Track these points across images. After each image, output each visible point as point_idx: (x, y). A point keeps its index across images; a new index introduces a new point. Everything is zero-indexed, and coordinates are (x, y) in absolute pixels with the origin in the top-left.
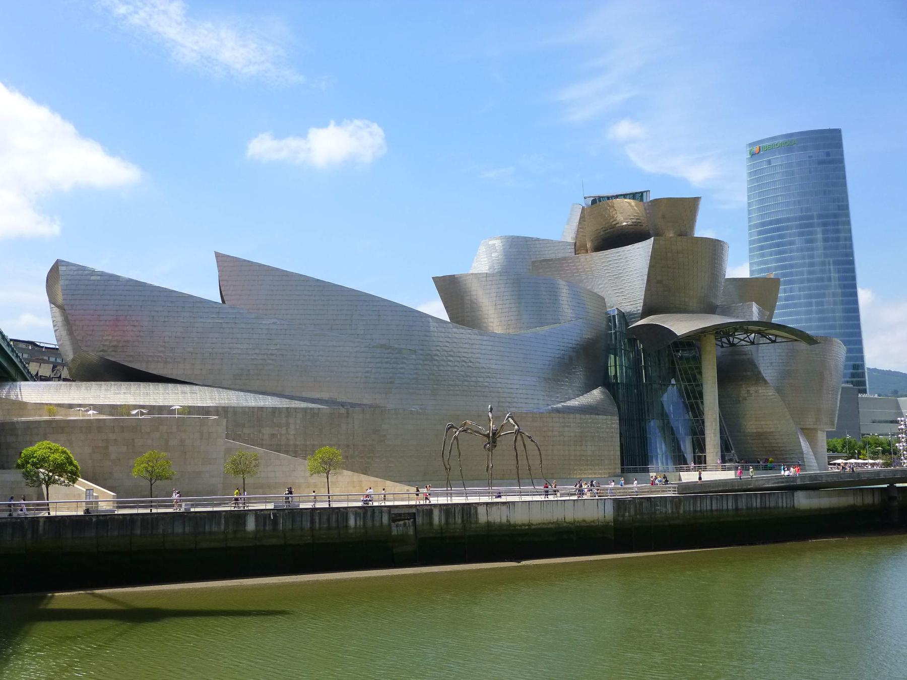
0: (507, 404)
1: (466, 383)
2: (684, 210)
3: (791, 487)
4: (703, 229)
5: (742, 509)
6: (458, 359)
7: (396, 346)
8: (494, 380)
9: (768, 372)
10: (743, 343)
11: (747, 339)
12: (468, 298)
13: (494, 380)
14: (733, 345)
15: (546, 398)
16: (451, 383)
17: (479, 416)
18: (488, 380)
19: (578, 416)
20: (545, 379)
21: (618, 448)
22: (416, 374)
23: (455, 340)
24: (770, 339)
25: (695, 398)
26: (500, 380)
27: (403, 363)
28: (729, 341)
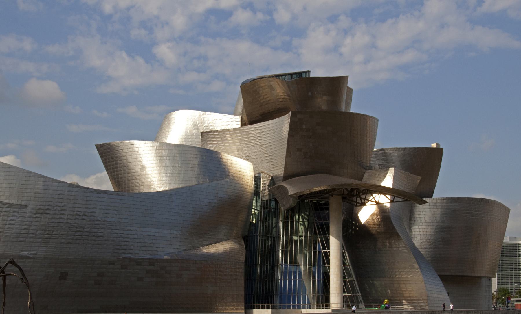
1: (79, 233)
7: (7, 201)
8: (110, 231)
12: (120, 162)
13: (110, 231)
18: (102, 230)
22: (26, 225)
27: (13, 216)
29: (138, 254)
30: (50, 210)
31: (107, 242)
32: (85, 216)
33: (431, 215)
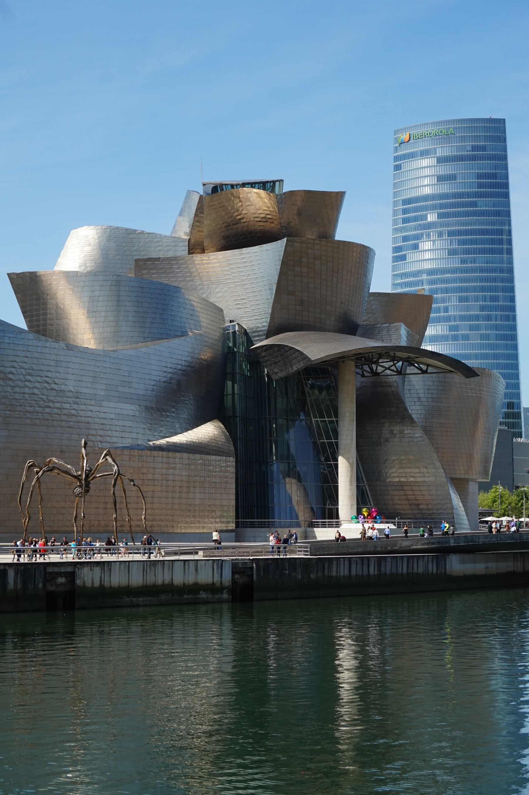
0: (99, 438)
1: (48, 410)
2: (322, 207)
3: (443, 549)
4: (344, 232)
5: (386, 574)
6: (39, 379)
8: (83, 407)
9: (415, 410)
10: (388, 372)
11: (393, 368)
13: (83, 407)
14: (376, 374)
15: (148, 432)
16: (30, 409)
17: (61, 452)
18: (75, 406)
19: (185, 455)
20: (147, 408)
21: (233, 497)
23: (37, 355)
24: (420, 369)
25: (328, 437)
26: (90, 408)
28: (372, 369)
29: (116, 443)
30: (14, 374)
31: (80, 424)
32: (55, 384)
33: (426, 391)
